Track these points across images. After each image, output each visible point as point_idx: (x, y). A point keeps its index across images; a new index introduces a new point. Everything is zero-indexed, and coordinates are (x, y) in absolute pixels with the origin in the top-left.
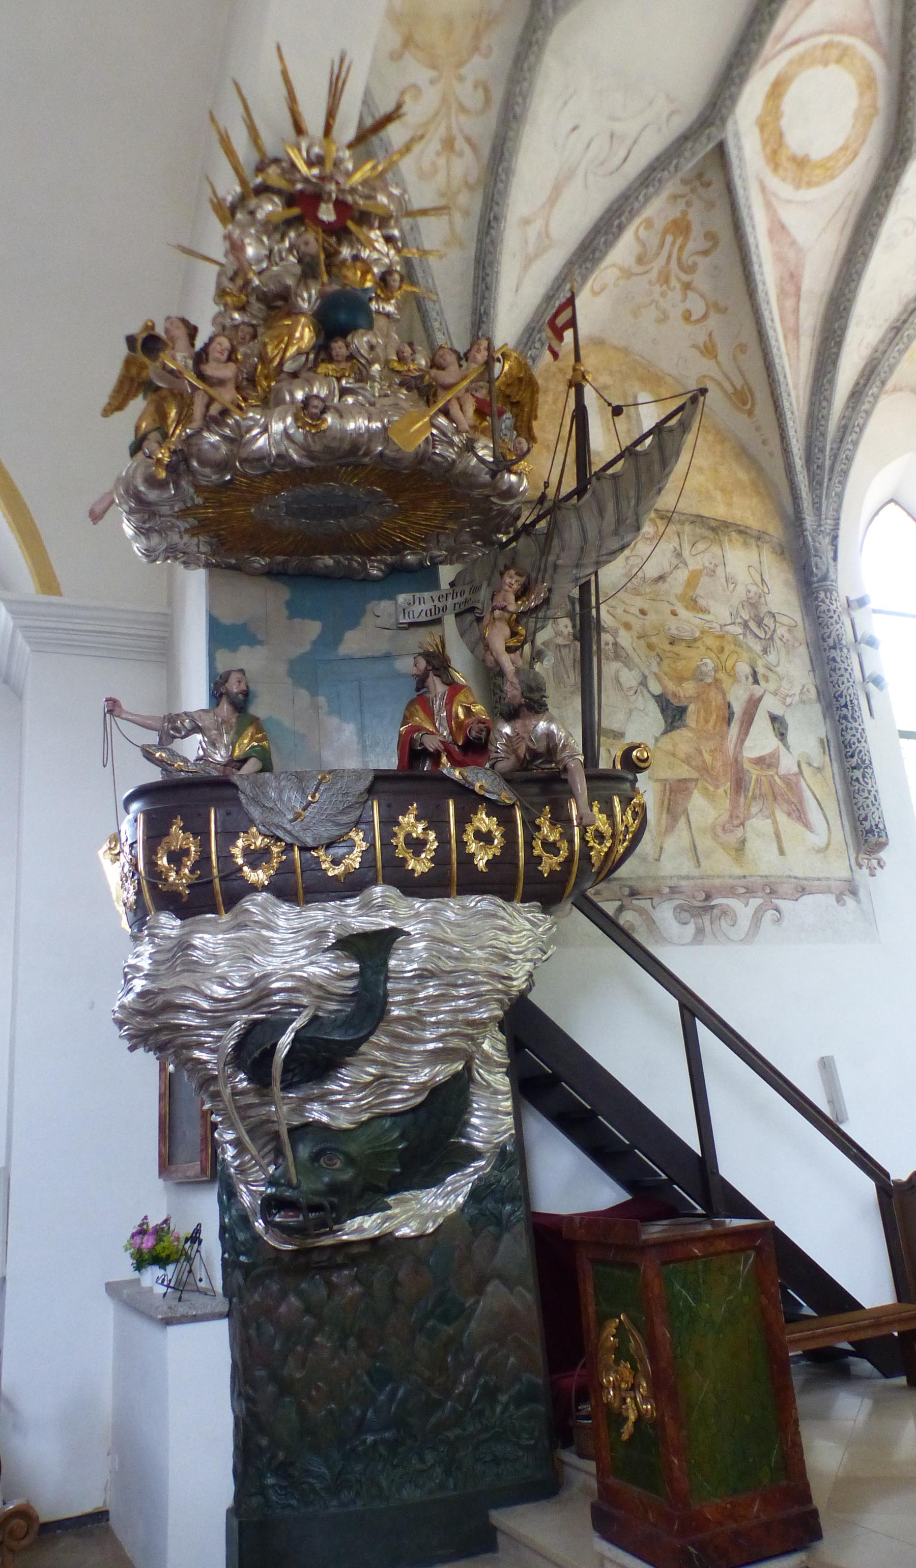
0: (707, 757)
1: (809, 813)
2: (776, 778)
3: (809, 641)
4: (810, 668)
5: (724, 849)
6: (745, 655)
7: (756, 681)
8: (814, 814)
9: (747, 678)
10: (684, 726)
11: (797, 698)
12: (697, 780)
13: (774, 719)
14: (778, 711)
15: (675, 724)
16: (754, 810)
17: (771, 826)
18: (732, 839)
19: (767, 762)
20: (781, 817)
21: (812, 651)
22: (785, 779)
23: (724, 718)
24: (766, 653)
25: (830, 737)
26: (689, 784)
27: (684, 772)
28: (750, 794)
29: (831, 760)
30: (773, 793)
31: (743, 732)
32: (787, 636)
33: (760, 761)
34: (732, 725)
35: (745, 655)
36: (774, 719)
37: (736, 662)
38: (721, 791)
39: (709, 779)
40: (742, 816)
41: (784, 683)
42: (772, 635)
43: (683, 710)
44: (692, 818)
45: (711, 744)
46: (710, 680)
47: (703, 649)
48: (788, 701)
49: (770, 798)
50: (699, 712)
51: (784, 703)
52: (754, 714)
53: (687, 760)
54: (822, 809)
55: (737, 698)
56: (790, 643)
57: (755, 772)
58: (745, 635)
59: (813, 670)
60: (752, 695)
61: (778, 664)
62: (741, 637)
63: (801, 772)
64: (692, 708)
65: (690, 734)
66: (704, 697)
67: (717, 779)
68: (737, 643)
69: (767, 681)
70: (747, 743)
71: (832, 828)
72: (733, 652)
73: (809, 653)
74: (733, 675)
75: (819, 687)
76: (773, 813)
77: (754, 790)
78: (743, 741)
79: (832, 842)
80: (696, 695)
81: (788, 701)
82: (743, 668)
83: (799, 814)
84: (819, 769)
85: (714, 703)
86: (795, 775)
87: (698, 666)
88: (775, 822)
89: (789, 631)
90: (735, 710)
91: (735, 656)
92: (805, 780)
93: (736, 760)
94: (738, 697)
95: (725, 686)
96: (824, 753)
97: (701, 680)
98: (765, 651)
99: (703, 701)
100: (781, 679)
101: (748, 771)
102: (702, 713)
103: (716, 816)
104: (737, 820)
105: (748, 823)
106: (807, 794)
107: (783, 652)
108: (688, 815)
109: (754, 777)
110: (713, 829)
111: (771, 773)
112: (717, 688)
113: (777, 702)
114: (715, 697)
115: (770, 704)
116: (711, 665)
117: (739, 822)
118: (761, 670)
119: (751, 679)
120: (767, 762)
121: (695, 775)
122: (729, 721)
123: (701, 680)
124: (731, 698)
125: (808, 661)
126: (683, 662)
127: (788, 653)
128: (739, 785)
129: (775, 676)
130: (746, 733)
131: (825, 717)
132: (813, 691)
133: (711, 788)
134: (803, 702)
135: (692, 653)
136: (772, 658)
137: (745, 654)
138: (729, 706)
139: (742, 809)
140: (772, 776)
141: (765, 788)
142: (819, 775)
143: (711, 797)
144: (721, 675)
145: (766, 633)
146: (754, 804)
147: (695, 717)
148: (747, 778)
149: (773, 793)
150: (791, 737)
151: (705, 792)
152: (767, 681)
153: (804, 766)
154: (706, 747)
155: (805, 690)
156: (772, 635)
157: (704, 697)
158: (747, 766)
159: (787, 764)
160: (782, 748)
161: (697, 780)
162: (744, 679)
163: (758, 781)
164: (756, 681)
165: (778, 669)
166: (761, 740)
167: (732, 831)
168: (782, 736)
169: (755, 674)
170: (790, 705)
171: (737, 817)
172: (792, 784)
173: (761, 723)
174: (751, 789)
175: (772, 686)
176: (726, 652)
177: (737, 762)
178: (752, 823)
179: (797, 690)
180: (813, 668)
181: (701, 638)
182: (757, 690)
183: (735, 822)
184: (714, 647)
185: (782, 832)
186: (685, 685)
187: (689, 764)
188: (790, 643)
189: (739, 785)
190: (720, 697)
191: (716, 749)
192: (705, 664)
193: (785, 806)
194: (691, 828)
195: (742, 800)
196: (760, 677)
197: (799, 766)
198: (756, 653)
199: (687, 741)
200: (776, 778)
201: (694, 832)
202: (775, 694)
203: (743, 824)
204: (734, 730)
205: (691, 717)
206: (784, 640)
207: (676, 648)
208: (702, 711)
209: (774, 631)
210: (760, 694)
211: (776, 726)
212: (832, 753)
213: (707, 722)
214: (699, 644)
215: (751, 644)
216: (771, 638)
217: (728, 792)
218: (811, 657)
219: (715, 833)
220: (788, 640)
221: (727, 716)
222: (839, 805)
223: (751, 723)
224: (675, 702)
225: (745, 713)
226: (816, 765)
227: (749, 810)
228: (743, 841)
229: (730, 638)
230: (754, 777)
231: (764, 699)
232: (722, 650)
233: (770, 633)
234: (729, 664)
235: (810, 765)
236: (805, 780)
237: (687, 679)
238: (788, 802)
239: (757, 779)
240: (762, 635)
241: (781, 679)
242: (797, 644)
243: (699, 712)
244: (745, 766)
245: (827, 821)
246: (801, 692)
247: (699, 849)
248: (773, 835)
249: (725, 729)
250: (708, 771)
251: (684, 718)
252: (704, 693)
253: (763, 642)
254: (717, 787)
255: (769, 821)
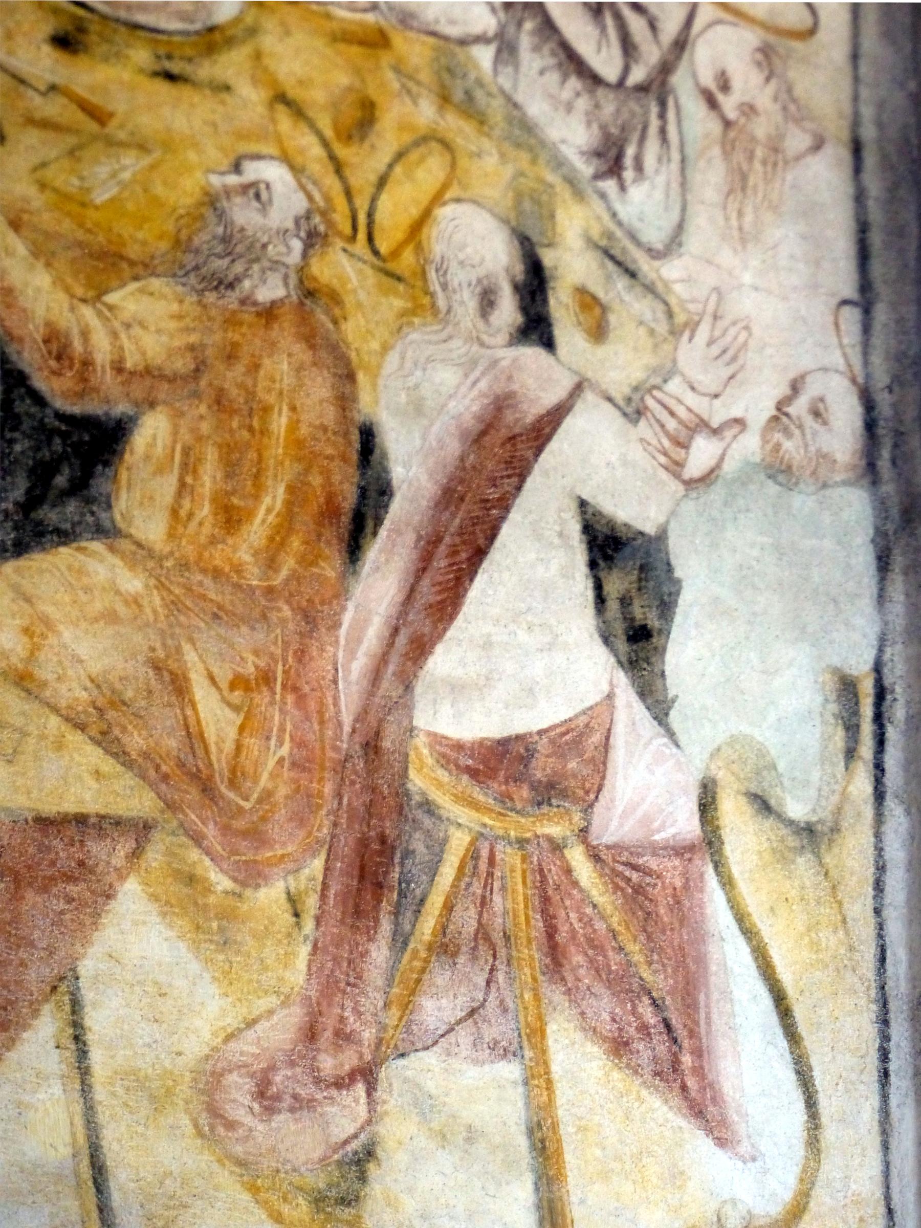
0: (215, 715)
1: (722, 1045)
2: (576, 856)
3: (869, 133)
4: (849, 290)
5: (254, 1190)
6: (492, 169)
7: (536, 328)
8: (748, 1058)
9: (487, 301)
10: (101, 531)
11: (749, 446)
12: (142, 830)
13: (606, 544)
14: (635, 507)
15: (50, 515)
16: (437, 1008)
17: (517, 1094)
18: (300, 1144)
19: (541, 768)
20: (578, 1061)
21: (874, 184)
22: (627, 870)
23: (330, 511)
24: (614, 168)
25: (897, 674)
26: (97, 849)
27: (79, 779)
28: (427, 926)
29: (879, 795)
30: (551, 932)
31: (427, 592)
32: (747, 83)
33: (499, 763)
34: (373, 553)
35: (492, 169)
36: (606, 544)
37: (438, 199)
38: (270, 896)
39: (211, 831)
40: (368, 1035)
41: (692, 355)
42: (666, 69)
43: (98, 443)
44: (98, 1022)
45: (247, 648)
46: (271, 290)
47: (251, 96)
48: (702, 454)
49: (531, 954)
50: (190, 465)
51: (675, 468)
52: (505, 504)
53: (101, 721)
54: (792, 1035)
55: (417, 408)
56: (761, 129)
57: (463, 814)
58: (506, 49)
59: (865, 298)
60: (501, 404)
61: (675, 241)
62: (484, 56)
63: (711, 841)
64: (152, 434)
65: (133, 583)
66: (232, 378)
67: (256, 836)
68: (454, 89)
69: (599, 332)
70: (443, 661)
71: (830, 1133)
72: (428, 138)
73: (860, 198)
74: (408, 274)
75: (884, 402)
76: (536, 1034)
77: (449, 907)
78: (421, 649)
79: (821, 1199)
80: (183, 364)
81: (702, 454)
82: (475, 243)
83: (670, 1048)
84: (811, 836)
85: (280, 422)
86: (683, 851)
87: (212, 201)
88: (538, 1078)
89: (766, 56)
90: (398, 473)
91: (430, 171)
92: (727, 883)
93: (372, 747)
94: (423, 400)
95: (352, 330)
96: (850, 754)
97: (225, 284)
98: (611, 159)
99: (220, 401)
100: (678, 327)
101: (428, 807)
102: (209, 477)
103: (232, 1021)
104: (338, 1048)
105: (393, 1073)
106: (730, 957)
107: (710, 178)
108: (76, 1005)
109: (459, 842)
110: (210, 1080)
111: (555, 830)
112: (310, 337)
113: (637, 453)
114: (286, 375)
115: (597, 461)
116: (286, 196)
117: (349, 1060)
118: (572, 265)
119: (508, 312)
120: (541, 768)
121: (133, 799)
122: (358, 526)
123: (225, 284)
124: (384, 404)
125: (842, 246)
126: (130, 164)
127: (739, 182)
128: (374, 871)
129: (642, 306)
130: (447, 605)
131: (883, 563)
132: (846, 415)
133: (221, 882)
134: (779, 471)
135: (177, 114)
136: (643, 202)
137: (491, 161)
138: (368, 439)
139: (372, 1000)
140: (557, 847)
141: (512, 902)
142: (804, 863)
143: (211, 926)
144: (341, 267)
145: (628, 47)
146: (440, 977)
147: (167, 486)
148: (418, 845)
149: (551, 932)
150: (687, 652)
151: (183, 895)
152: (599, 332)
153: (733, 812)
154: (206, 662)
155: (799, 407)
156: (666, 69)
157: (232, 378)
158: (425, 779)
159: (646, 791)
160: (629, 708)
161: (142, 830)
162: (467, 305)
163: (479, 864)
164: (536, 328)
165: (671, 271)
166: (520, 652)
167: (300, 1105)
168: (638, 641)
169: (534, 284)
170: (707, 479)
171: (344, 1037)
172: (655, 894)
173: (533, 567)
174: (436, 901)
175: (620, 363)
176: (387, 138)
177: (375, 748)
178: (421, 1073)
179: (756, 401)
180: (865, 286)
181: (253, 32)
182: (538, 378)
183: (328, 1064)
184: (316, 97)
185: (567, 1130)
186: (126, 299)
187: (106, 741)
188: (761, 129)
189: (374, 871)
190: (319, 390)
191: (266, 678)
192: (256, 192)
193: (604, 1006)
194: (84, 1072)
195: (379, 953)
196: (560, 305)
197: (707, 805)
198: (559, 163)
199: (111, 617)
200: (576, 856)
201: (100, 1094)
202: (633, 410)
203: (367, 1075)
204: (380, 583)
205: (144, 491)
206: (729, 104)
207: (87, 76)
208: (211, 455)
209: (681, 45)
210: (550, 398)
211: (615, 585)
212: (893, 759)
213: (231, 518)
214: (230, 65)
215: (536, 108)
216: (658, 88)
217: (311, 903)
218: (863, 228)
219: (214, 1112)
220: (749, 110)
221: (348, 498)
222: (884, 1022)
223: (480, 554)
224: (57, 390)
225: (449, 496)
226: (797, 810)
227: (407, 1005)
228: (361, 1160)
229: (414, 51)
230: (459, 842)
231: (571, 424)
232: (363, 119)
233: (651, 54)
234: (394, 210)
235: (763, 805)
236: (727, 883)
237: (144, 268)
238: (624, 985)
239: (473, 854)
240: (606, 62)
241: (675, 332)
242: (797, 141)
243: (190, 465)
244: (417, 781)
245: (811, 1103)
246: (780, 416)
247: (120, 1180)
248: (522, 1142)
249: (331, 566)
250: (207, 789)
251: (99, 485)
252: (231, 356)
253: (609, 105)
254: (251, 875)
255: (511, 1070)
